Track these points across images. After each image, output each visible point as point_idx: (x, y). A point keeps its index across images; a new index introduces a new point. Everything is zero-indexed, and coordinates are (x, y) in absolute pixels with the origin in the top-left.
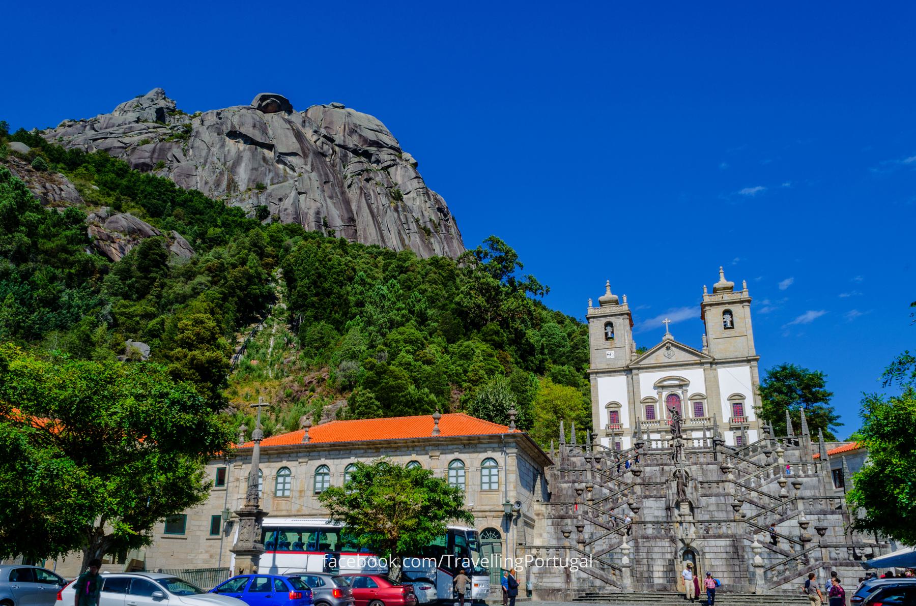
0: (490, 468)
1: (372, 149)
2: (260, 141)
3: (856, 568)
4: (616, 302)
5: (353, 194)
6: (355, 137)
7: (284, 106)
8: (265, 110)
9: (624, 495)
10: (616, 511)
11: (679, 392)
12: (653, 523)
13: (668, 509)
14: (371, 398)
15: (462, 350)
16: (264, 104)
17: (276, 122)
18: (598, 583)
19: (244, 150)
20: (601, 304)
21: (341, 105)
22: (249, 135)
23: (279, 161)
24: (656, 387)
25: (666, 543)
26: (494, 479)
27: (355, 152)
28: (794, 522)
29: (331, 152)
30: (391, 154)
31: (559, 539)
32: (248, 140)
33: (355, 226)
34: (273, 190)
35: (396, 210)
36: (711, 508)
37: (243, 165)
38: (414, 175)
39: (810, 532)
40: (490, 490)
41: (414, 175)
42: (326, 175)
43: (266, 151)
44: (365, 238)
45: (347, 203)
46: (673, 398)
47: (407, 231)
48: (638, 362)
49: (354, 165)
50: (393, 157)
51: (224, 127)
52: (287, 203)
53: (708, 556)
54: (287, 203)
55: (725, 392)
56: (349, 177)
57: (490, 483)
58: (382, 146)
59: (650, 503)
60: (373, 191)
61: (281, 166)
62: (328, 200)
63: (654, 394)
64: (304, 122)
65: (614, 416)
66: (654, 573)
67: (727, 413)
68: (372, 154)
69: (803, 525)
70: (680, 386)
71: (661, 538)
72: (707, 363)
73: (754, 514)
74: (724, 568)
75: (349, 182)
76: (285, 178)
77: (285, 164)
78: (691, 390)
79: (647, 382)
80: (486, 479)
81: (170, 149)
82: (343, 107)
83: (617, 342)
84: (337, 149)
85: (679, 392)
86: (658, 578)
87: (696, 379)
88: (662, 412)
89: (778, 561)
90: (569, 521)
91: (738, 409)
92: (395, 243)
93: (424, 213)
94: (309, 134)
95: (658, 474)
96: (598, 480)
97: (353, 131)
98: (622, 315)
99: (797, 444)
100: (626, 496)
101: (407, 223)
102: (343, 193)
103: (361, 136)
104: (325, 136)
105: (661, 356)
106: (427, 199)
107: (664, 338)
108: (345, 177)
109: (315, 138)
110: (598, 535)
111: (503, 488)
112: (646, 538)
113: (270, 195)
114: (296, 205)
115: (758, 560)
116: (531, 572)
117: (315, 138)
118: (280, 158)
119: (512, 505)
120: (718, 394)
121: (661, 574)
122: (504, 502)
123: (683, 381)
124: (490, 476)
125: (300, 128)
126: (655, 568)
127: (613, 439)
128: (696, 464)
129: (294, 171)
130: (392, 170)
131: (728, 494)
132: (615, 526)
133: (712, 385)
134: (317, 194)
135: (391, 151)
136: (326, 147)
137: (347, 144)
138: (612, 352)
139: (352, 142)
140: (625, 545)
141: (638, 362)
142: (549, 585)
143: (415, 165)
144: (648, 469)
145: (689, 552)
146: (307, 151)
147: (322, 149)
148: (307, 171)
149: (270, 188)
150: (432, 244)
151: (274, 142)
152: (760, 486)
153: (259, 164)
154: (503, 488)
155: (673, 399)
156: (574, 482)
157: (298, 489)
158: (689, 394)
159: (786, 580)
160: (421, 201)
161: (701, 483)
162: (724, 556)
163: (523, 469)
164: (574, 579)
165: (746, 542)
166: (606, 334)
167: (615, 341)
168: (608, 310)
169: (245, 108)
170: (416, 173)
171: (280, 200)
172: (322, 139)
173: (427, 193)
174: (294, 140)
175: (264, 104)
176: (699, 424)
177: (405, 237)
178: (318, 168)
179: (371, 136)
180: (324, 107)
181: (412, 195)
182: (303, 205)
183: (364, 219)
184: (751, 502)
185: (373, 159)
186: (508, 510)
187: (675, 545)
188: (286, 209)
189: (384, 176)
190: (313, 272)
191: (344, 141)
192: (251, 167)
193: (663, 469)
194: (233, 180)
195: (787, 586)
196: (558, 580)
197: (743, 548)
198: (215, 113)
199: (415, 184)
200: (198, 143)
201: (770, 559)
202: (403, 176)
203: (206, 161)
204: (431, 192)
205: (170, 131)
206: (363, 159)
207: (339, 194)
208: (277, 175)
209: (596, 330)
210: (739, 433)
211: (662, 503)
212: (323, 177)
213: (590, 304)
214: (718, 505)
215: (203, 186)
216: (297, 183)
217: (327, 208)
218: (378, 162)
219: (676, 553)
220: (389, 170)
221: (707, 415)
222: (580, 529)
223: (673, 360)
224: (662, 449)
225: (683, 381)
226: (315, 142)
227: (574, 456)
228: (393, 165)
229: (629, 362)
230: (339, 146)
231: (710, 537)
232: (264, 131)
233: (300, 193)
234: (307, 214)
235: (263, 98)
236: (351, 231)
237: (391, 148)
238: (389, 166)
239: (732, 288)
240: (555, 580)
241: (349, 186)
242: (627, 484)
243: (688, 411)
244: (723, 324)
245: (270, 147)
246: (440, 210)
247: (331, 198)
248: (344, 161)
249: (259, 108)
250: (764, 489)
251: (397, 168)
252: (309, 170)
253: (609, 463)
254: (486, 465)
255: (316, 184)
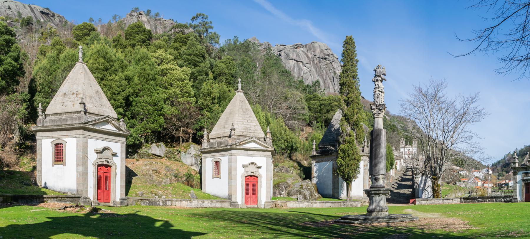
58: (329, 55)
87: (411, 149)
88: (407, 152)
91: (415, 152)
105: (407, 146)
108: (321, 68)
125: (306, 52)
130: (333, 63)
135: (332, 56)
139: (322, 55)
220: (332, 63)
230: (318, 57)
238: (332, 62)
247: (319, 76)
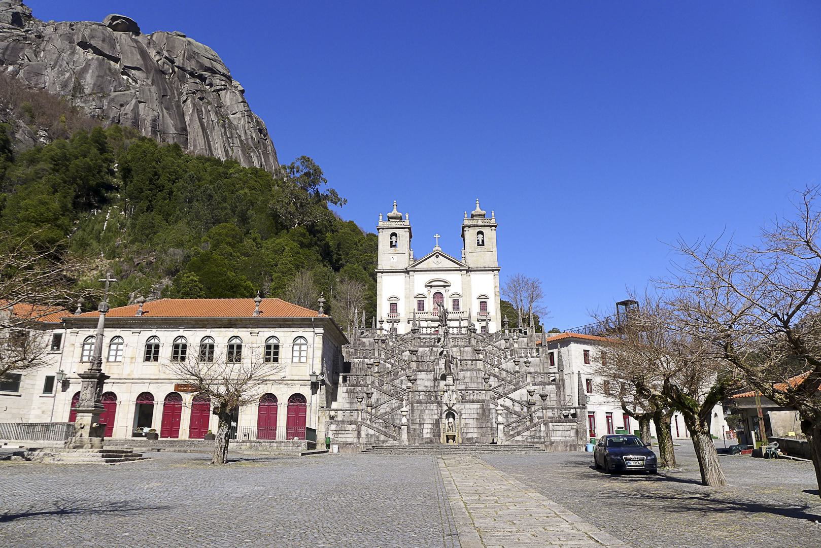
0: (301, 345)
1: (207, 74)
2: (108, 53)
3: (565, 424)
4: (401, 219)
5: (189, 108)
6: (193, 62)
7: (131, 27)
8: (115, 28)
9: (402, 369)
10: (396, 382)
11: (442, 290)
12: (425, 391)
13: (435, 380)
14: (196, 281)
15: (274, 247)
16: (115, 23)
17: (123, 37)
18: (382, 438)
19: (93, 59)
20: (389, 218)
21: (183, 34)
22: (98, 47)
23: (123, 74)
24: (427, 286)
25: (434, 407)
26: (304, 354)
27: (192, 74)
28: (524, 391)
29: (171, 71)
30: (223, 80)
31: (351, 403)
32: (97, 51)
33: (187, 135)
34: (116, 96)
35: (223, 126)
36: (466, 380)
37: (90, 71)
38: (241, 100)
39: (536, 397)
40: (300, 363)
41: (241, 100)
42: (165, 89)
43: (112, 63)
44: (195, 146)
45: (182, 115)
46: (438, 295)
47: (231, 145)
48: (414, 266)
49: (189, 85)
50: (224, 83)
51: (75, 37)
52: (129, 108)
53: (464, 416)
54: (129, 108)
55: (476, 293)
56: (184, 93)
57: (300, 357)
59: (422, 375)
60: (205, 108)
61: (125, 77)
62: (164, 110)
63: (424, 291)
64: (149, 43)
65: (394, 306)
66: (424, 430)
67: (476, 308)
68: (206, 78)
69: (531, 393)
70: (444, 286)
71: (431, 403)
72: (464, 270)
73: (496, 385)
74: (475, 426)
75: (185, 99)
76: (128, 88)
77: (129, 76)
78: (452, 290)
79: (420, 281)
80: (296, 354)
81: (22, 49)
82: (184, 36)
83: (399, 249)
84: (176, 69)
85: (442, 290)
86: (427, 433)
87: (455, 279)
88: (429, 305)
89: (513, 420)
90: (360, 388)
91: (483, 306)
92: (220, 153)
93: (247, 131)
94: (152, 53)
95: (428, 353)
96: (383, 356)
97: (192, 55)
98: (404, 228)
99: (526, 333)
100: (404, 370)
101: (232, 137)
102: (178, 107)
103: (198, 62)
104: (166, 58)
105: (432, 263)
106: (250, 120)
107: (434, 249)
108: (182, 93)
109: (158, 58)
110: (382, 401)
111: (310, 361)
112: (419, 402)
113: (113, 100)
114: (135, 110)
115: (500, 419)
116: (330, 429)
117: (158, 58)
118: (125, 71)
119: (317, 376)
120: (470, 294)
121: (429, 431)
122: (311, 373)
123: (446, 283)
124: (300, 351)
126: (425, 426)
127: (393, 325)
128: (456, 346)
129: (136, 83)
130: (222, 93)
131: (479, 370)
132: (396, 394)
133: (467, 286)
134: (156, 105)
135: (223, 78)
136: (166, 67)
137: (185, 66)
138: (395, 257)
140: (404, 409)
141: (414, 266)
142: (344, 440)
143: (242, 92)
144: (421, 349)
145: (450, 414)
146: (149, 67)
147: (163, 67)
148: (147, 84)
149: (113, 94)
150: (251, 157)
151: (121, 56)
152: (501, 364)
153: (105, 73)
154: (310, 361)
155: (438, 295)
156: (365, 358)
157: (130, 356)
158: (450, 293)
159: (518, 433)
160: (245, 121)
161: (461, 361)
162: (476, 416)
163: (327, 346)
164: (363, 434)
165: (492, 406)
166: (391, 242)
167: (398, 249)
168: (394, 223)
169: (96, 24)
170: (243, 98)
171: (122, 105)
172: (163, 59)
173: (250, 116)
174: (139, 57)
175: (115, 23)
176: (456, 316)
177: (229, 149)
178: (158, 83)
179: (207, 63)
180: (168, 34)
181: (237, 115)
182: (141, 113)
183: (194, 131)
184: (495, 376)
185: (207, 81)
186: (314, 379)
187: (440, 408)
188: (126, 114)
189: (215, 97)
190: (149, 170)
191: (183, 64)
192: (97, 73)
193: (432, 349)
194: (79, 84)
195: (519, 438)
196: (351, 436)
197: (489, 410)
198: (68, 25)
199: (241, 107)
200: (50, 47)
201: (507, 418)
202: (231, 99)
203: (56, 64)
204: (254, 115)
205: (24, 34)
206: (198, 81)
207: (174, 107)
208: (120, 84)
209: (384, 239)
210: (484, 324)
211: (431, 376)
212: (162, 91)
213: (381, 218)
214: (471, 378)
215: (51, 85)
216: (137, 93)
217: (163, 117)
218: (211, 85)
219: (441, 414)
220: (220, 93)
221: (461, 310)
222: (369, 395)
223: (440, 266)
224: (431, 334)
225: (446, 283)
226: (157, 61)
227: (364, 338)
228: (224, 90)
229: (407, 265)
230: (178, 67)
231: (467, 402)
232: (113, 47)
233: (140, 102)
234: (144, 120)
235: (114, 18)
236: (182, 139)
237: (223, 75)
238: (221, 90)
239: (484, 215)
240: (348, 436)
241: (185, 102)
242: (405, 361)
243: (448, 305)
244: (477, 242)
245: (117, 60)
246: (260, 131)
248: (182, 80)
249: (110, 26)
250: (504, 366)
251: (227, 92)
252: (150, 83)
253: (391, 344)
254: (297, 342)
255: (155, 96)
